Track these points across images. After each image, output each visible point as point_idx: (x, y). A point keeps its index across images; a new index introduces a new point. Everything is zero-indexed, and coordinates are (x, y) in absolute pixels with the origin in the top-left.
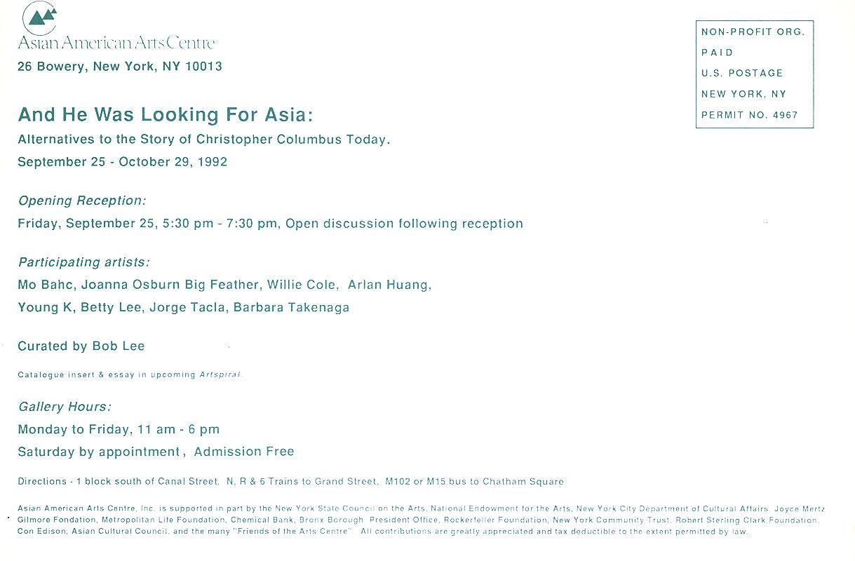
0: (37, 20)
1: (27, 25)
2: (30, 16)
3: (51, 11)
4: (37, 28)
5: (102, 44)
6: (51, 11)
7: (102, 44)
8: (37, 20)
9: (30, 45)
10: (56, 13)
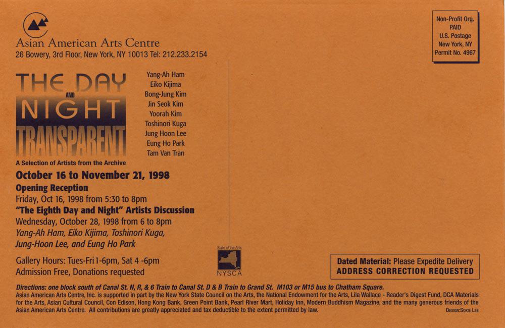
0: (34, 26)
1: (27, 31)
2: (28, 23)
3: (44, 20)
4: (33, 33)
5: (76, 44)
6: (44, 20)
7: (76, 44)
8: (34, 26)
9: (24, 44)
10: (48, 21)
